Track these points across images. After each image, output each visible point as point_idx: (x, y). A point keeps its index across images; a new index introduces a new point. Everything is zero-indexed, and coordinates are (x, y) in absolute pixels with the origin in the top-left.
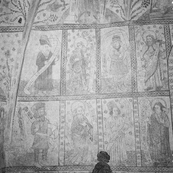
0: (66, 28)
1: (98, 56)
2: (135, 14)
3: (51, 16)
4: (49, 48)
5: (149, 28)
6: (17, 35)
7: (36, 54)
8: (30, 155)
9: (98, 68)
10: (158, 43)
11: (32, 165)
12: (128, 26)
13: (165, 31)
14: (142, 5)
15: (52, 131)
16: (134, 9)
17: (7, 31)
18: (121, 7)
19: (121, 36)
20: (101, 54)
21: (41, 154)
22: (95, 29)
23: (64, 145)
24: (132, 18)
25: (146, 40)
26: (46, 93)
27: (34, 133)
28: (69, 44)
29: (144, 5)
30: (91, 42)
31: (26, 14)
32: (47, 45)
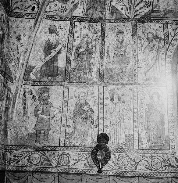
0: (73, 20)
1: (103, 47)
2: (138, 13)
3: (61, 7)
4: (57, 37)
5: (150, 26)
6: (29, 22)
7: (45, 42)
8: (30, 135)
9: (102, 58)
10: (158, 40)
11: (33, 144)
12: (131, 23)
13: (164, 30)
14: (144, 5)
15: (55, 114)
16: (137, 8)
17: (21, 17)
18: (126, 5)
19: (125, 32)
20: (105, 46)
21: (43, 135)
22: (100, 24)
23: (65, 127)
24: (135, 16)
25: (147, 36)
26: (51, 79)
27: (36, 115)
28: (76, 35)
29: (146, 6)
30: (96, 35)
31: (39, 2)
32: (55, 34)
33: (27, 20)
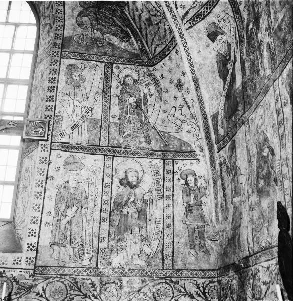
4: (225, 37)
7: (214, 61)
17: (167, 54)
32: (220, 37)
33: (174, 52)
